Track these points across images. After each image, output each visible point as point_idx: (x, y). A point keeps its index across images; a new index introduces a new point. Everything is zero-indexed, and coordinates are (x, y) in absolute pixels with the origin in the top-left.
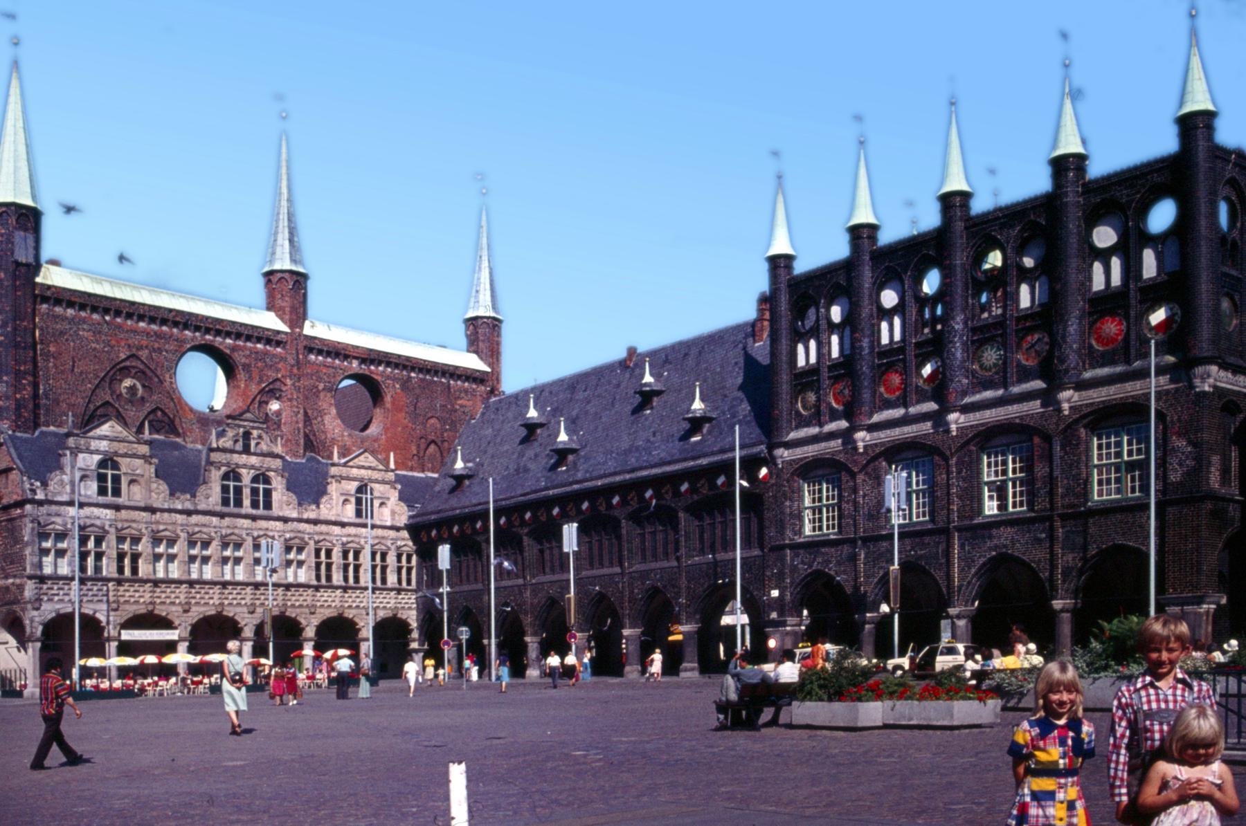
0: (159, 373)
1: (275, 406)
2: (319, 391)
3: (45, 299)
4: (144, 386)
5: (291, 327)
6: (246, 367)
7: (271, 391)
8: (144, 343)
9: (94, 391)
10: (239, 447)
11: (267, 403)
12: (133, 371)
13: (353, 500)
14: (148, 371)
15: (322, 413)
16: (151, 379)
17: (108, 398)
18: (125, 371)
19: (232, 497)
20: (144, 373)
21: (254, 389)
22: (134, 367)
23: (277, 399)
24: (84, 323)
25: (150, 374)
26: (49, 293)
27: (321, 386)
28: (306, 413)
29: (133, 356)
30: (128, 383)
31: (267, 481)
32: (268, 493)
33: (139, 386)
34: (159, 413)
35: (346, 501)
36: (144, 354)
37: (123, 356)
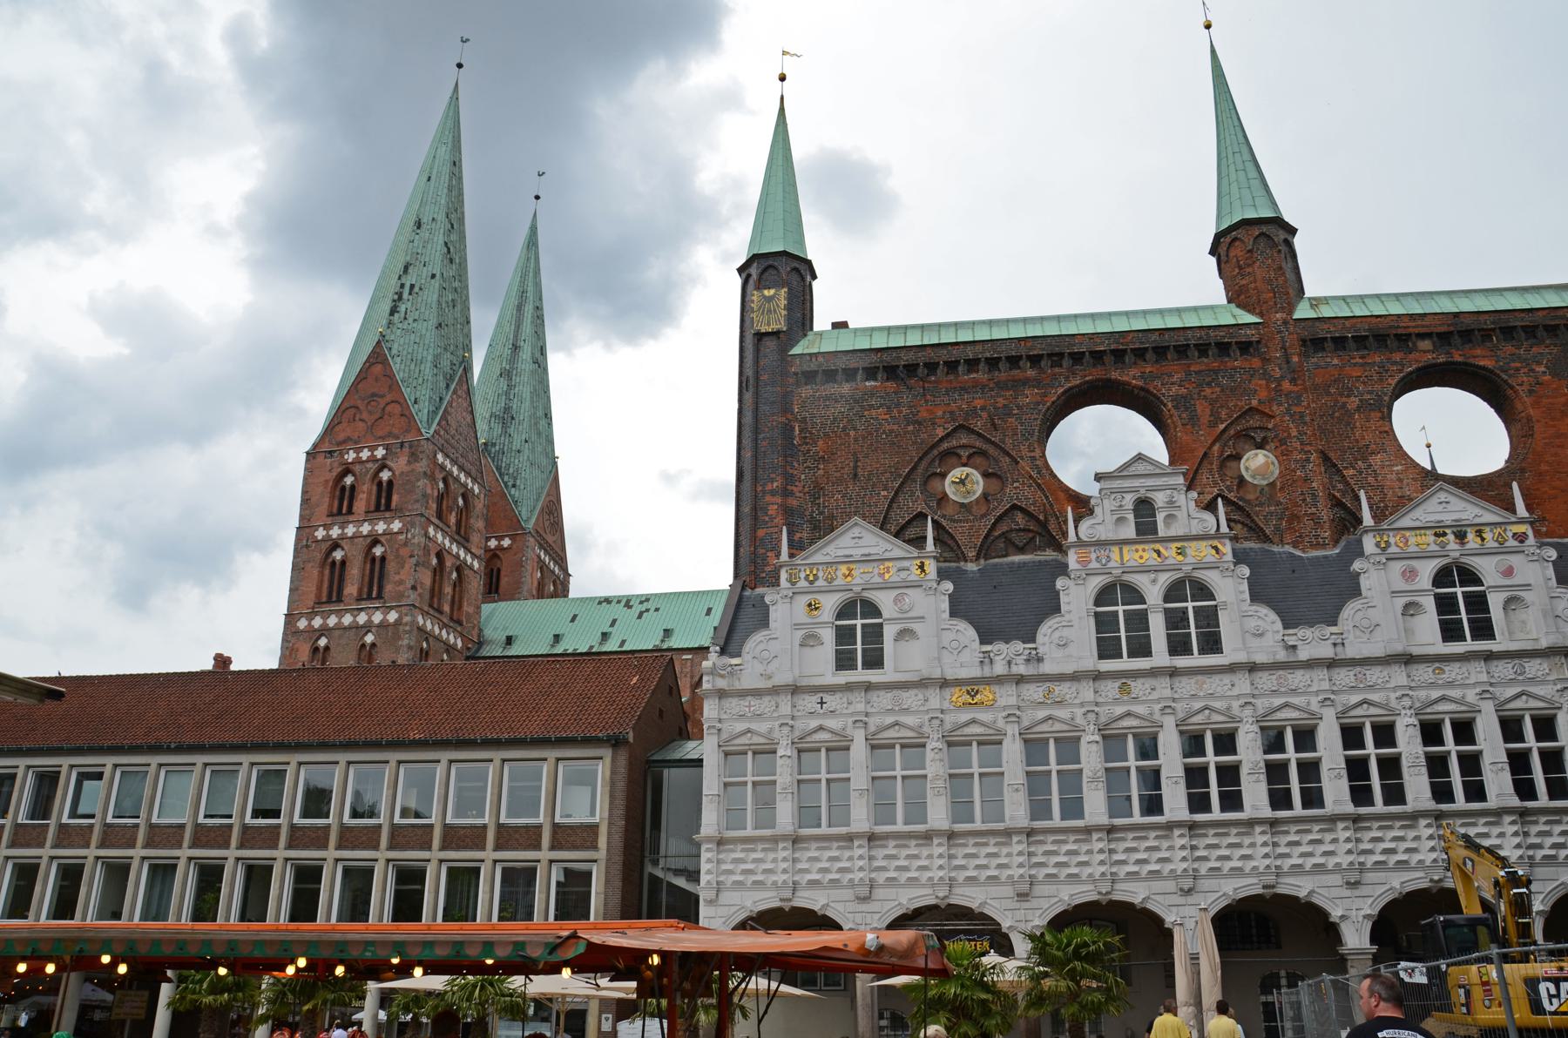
0: (1008, 444)
1: (1257, 463)
2: (1351, 416)
3: (810, 377)
4: (986, 475)
5: (1261, 315)
6: (1182, 402)
7: (1238, 435)
8: (978, 403)
9: (892, 501)
10: (1129, 531)
11: (1238, 457)
12: (964, 453)
13: (1429, 603)
14: (991, 450)
15: (1364, 453)
16: (997, 461)
17: (920, 507)
18: (950, 457)
19: (1120, 630)
20: (983, 453)
21: (1204, 436)
22: (964, 446)
23: (1260, 446)
24: (872, 395)
25: (991, 450)
26: (813, 367)
27: (1353, 402)
28: (1326, 458)
29: (961, 426)
30: (957, 473)
31: (1203, 591)
32: (1209, 618)
33: (976, 476)
34: (1020, 518)
35: (1411, 609)
36: (978, 425)
37: (940, 432)
